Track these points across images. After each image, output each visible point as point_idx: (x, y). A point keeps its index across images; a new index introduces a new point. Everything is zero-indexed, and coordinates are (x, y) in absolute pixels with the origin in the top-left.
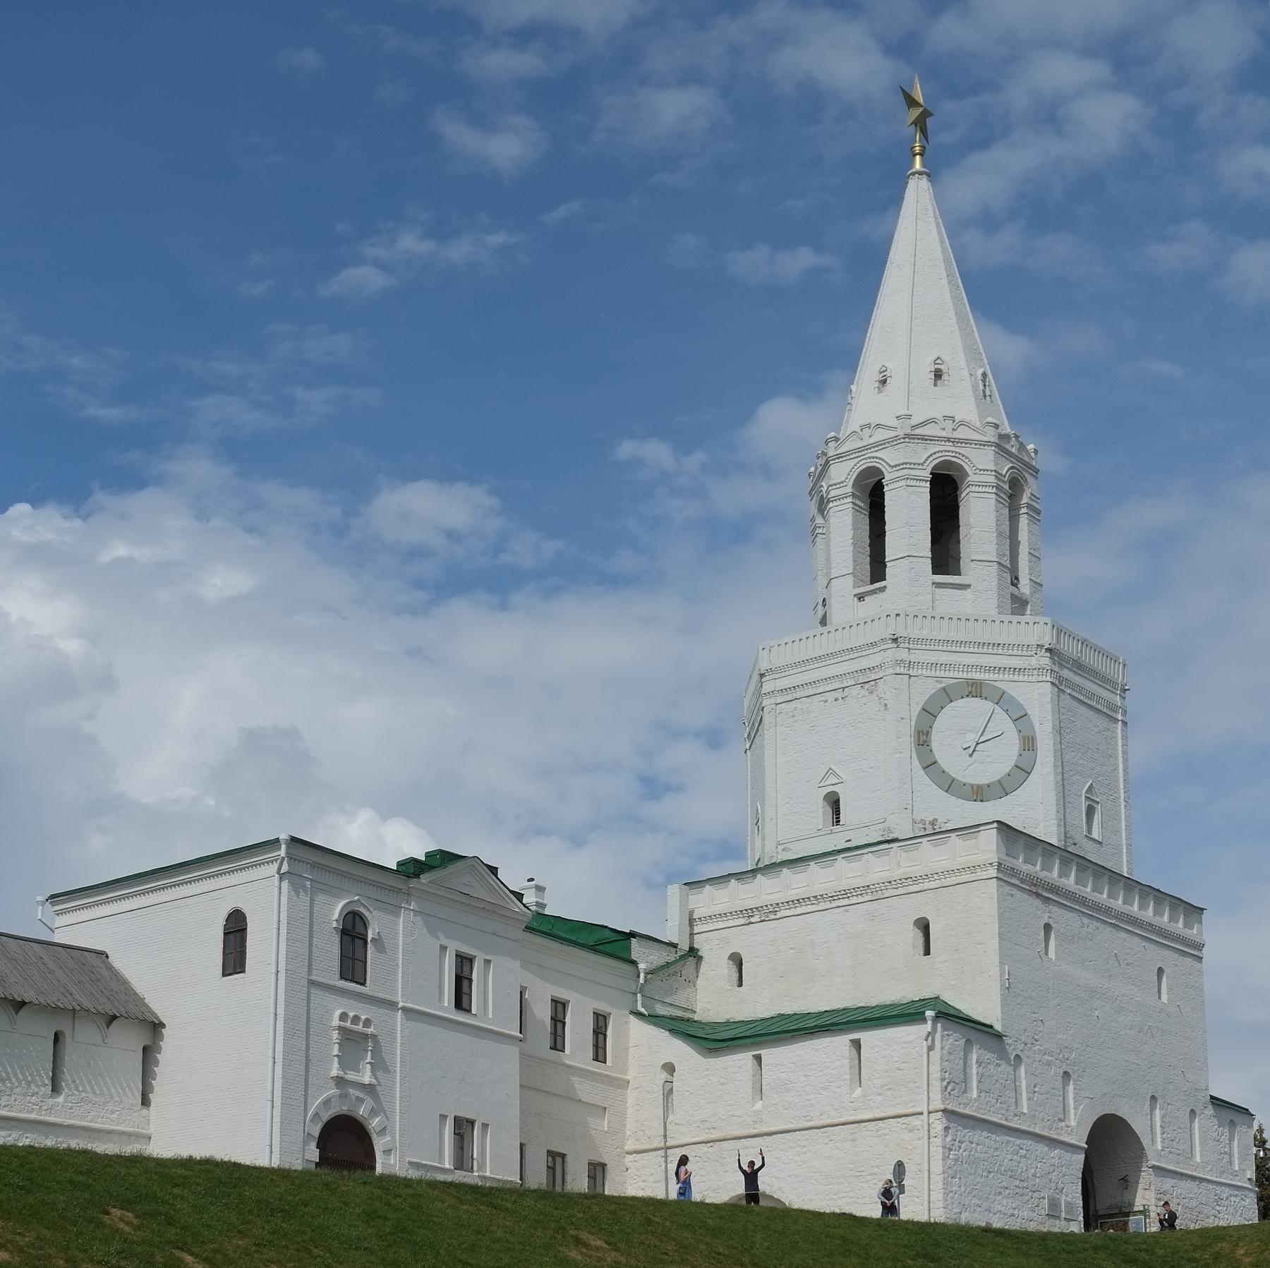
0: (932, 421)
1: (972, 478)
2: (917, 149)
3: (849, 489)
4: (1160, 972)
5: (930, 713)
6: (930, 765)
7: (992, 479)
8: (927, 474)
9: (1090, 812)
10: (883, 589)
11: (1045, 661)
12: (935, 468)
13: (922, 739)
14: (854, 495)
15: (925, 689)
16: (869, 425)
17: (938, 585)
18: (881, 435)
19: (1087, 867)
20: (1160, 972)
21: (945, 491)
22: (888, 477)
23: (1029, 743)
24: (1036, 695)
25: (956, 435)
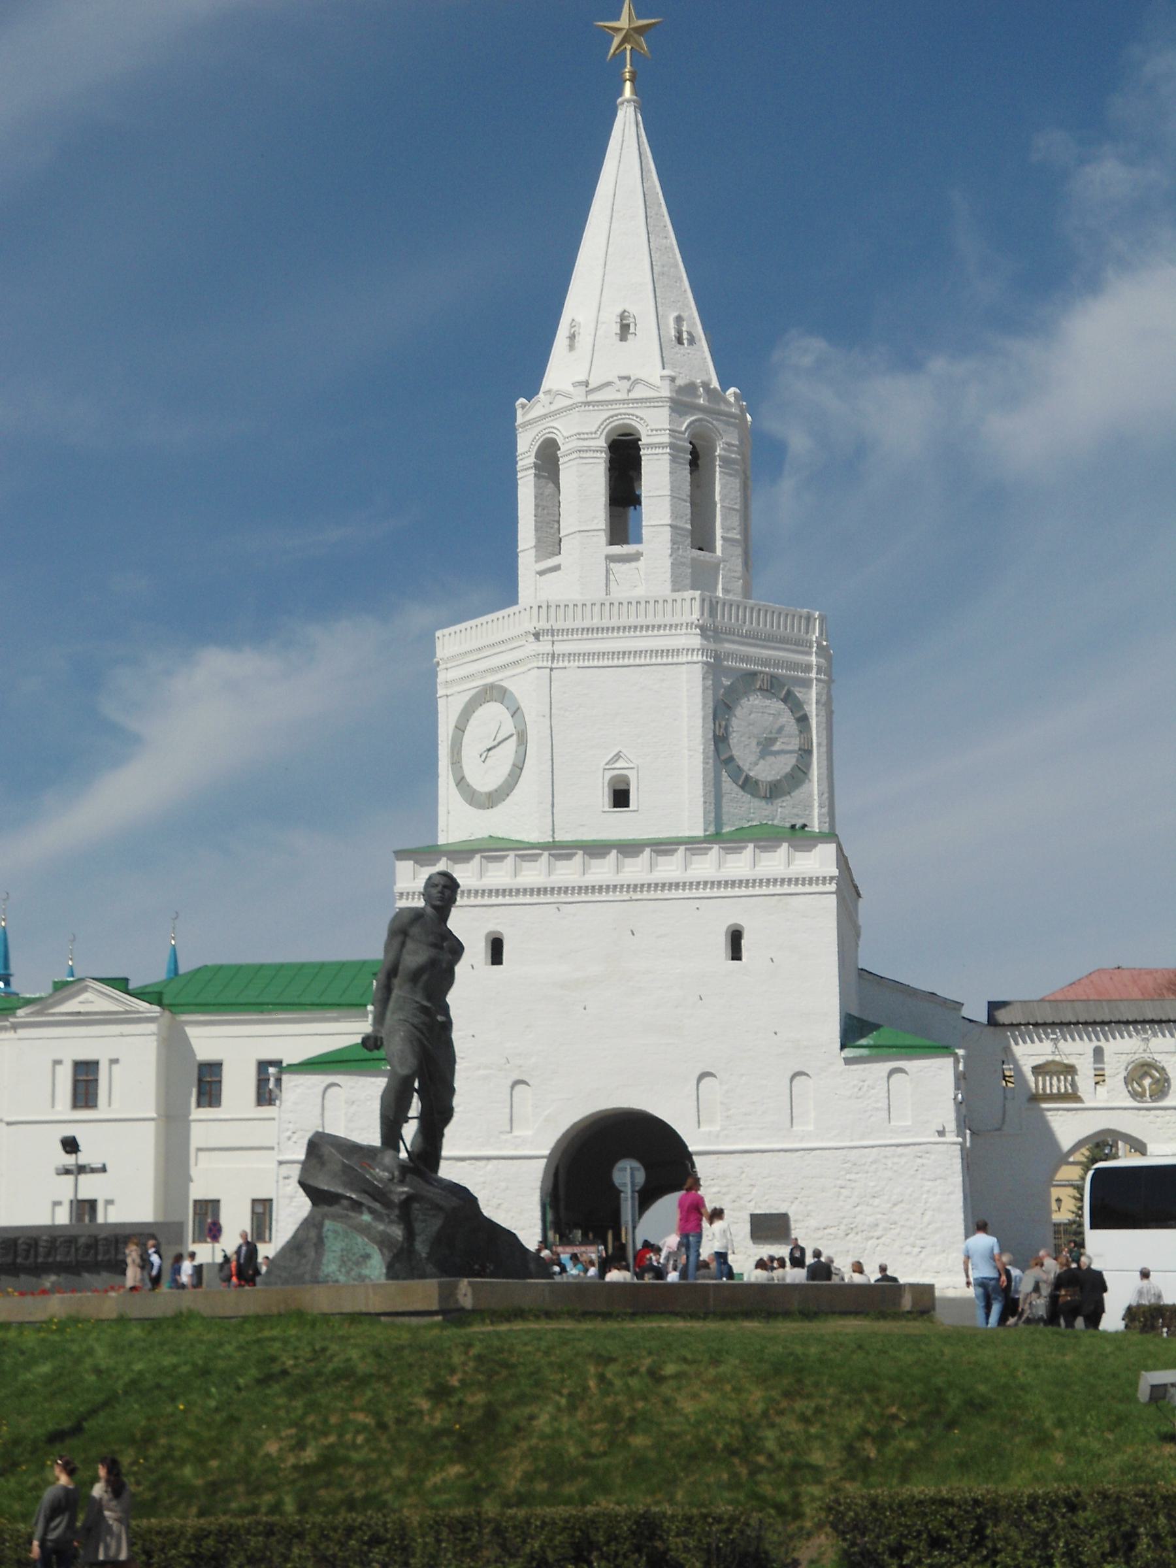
3: (602, 443)
10: (636, 557)
16: (628, 378)
18: (639, 392)
22: (644, 440)
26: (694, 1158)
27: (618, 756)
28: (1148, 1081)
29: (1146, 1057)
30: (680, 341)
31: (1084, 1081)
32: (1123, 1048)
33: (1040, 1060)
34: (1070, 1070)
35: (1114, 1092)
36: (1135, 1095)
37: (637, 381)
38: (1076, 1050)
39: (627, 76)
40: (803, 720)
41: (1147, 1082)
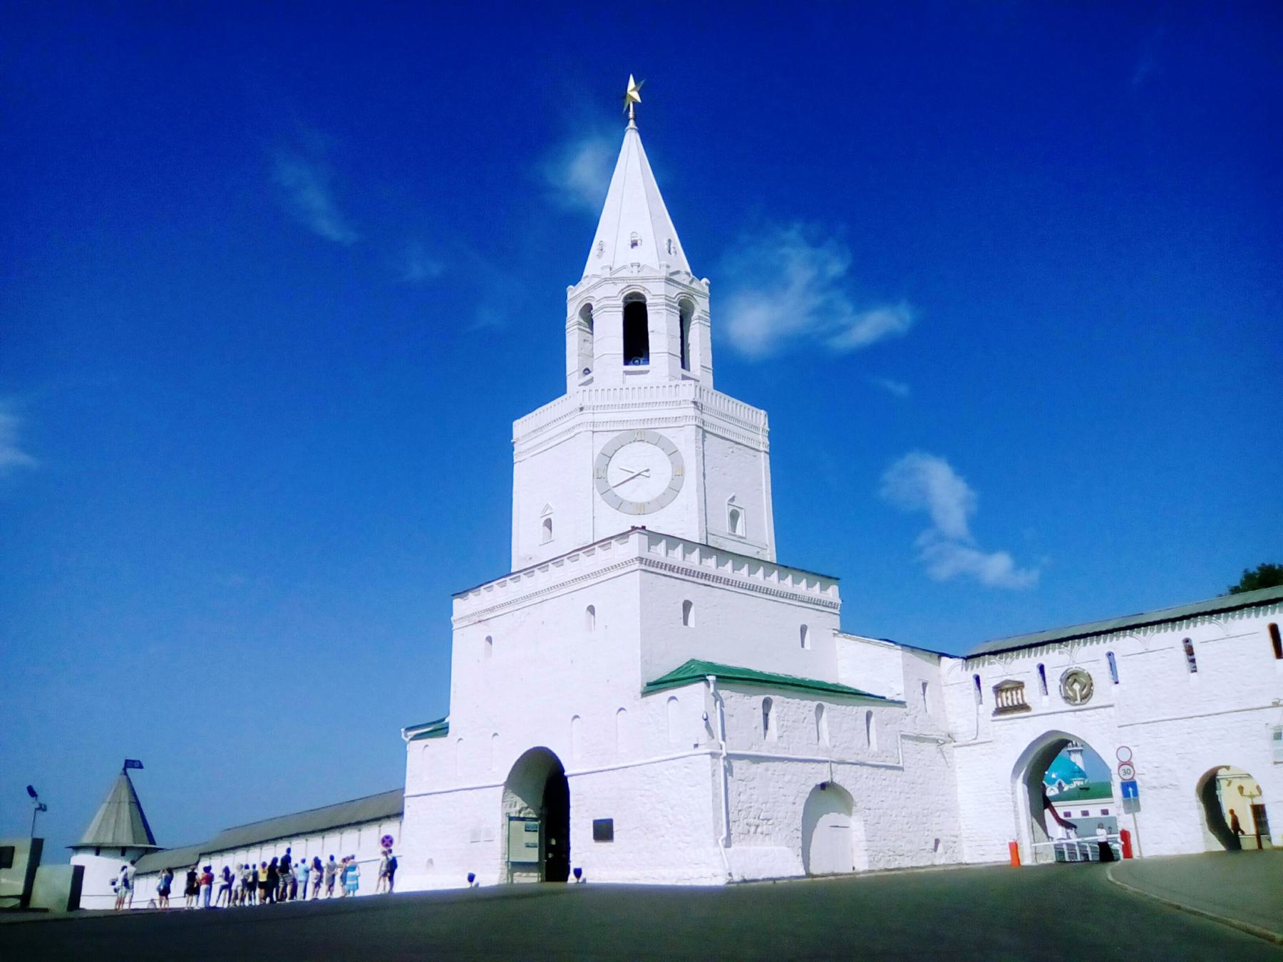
0: (624, 267)
1: (648, 302)
2: (631, 115)
4: (803, 630)
5: (607, 456)
6: (607, 492)
7: (663, 301)
8: (620, 303)
9: (734, 516)
10: (591, 380)
11: (691, 411)
12: (626, 298)
13: (600, 475)
14: (580, 324)
15: (602, 441)
17: (627, 373)
19: (723, 555)
20: (803, 630)
21: (635, 314)
23: (679, 474)
24: (685, 439)
25: (641, 274)
26: (569, 780)
27: (547, 507)
28: (1077, 686)
29: (1074, 668)
30: (634, 244)
31: (1031, 693)
32: (1057, 660)
33: (997, 682)
34: (1019, 685)
35: (1054, 699)
36: (1067, 698)
37: (594, 276)
38: (1021, 667)
39: (631, 115)
40: (673, 453)
41: (1077, 687)
